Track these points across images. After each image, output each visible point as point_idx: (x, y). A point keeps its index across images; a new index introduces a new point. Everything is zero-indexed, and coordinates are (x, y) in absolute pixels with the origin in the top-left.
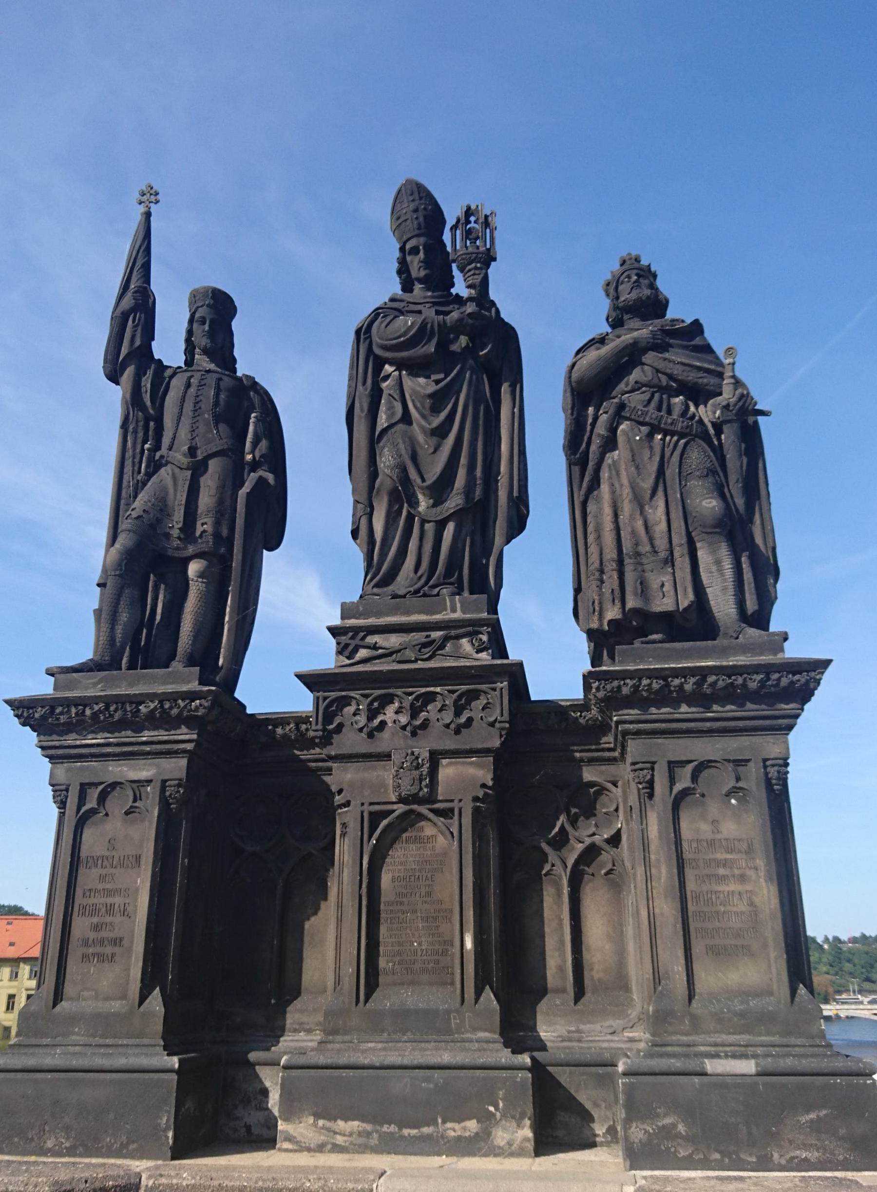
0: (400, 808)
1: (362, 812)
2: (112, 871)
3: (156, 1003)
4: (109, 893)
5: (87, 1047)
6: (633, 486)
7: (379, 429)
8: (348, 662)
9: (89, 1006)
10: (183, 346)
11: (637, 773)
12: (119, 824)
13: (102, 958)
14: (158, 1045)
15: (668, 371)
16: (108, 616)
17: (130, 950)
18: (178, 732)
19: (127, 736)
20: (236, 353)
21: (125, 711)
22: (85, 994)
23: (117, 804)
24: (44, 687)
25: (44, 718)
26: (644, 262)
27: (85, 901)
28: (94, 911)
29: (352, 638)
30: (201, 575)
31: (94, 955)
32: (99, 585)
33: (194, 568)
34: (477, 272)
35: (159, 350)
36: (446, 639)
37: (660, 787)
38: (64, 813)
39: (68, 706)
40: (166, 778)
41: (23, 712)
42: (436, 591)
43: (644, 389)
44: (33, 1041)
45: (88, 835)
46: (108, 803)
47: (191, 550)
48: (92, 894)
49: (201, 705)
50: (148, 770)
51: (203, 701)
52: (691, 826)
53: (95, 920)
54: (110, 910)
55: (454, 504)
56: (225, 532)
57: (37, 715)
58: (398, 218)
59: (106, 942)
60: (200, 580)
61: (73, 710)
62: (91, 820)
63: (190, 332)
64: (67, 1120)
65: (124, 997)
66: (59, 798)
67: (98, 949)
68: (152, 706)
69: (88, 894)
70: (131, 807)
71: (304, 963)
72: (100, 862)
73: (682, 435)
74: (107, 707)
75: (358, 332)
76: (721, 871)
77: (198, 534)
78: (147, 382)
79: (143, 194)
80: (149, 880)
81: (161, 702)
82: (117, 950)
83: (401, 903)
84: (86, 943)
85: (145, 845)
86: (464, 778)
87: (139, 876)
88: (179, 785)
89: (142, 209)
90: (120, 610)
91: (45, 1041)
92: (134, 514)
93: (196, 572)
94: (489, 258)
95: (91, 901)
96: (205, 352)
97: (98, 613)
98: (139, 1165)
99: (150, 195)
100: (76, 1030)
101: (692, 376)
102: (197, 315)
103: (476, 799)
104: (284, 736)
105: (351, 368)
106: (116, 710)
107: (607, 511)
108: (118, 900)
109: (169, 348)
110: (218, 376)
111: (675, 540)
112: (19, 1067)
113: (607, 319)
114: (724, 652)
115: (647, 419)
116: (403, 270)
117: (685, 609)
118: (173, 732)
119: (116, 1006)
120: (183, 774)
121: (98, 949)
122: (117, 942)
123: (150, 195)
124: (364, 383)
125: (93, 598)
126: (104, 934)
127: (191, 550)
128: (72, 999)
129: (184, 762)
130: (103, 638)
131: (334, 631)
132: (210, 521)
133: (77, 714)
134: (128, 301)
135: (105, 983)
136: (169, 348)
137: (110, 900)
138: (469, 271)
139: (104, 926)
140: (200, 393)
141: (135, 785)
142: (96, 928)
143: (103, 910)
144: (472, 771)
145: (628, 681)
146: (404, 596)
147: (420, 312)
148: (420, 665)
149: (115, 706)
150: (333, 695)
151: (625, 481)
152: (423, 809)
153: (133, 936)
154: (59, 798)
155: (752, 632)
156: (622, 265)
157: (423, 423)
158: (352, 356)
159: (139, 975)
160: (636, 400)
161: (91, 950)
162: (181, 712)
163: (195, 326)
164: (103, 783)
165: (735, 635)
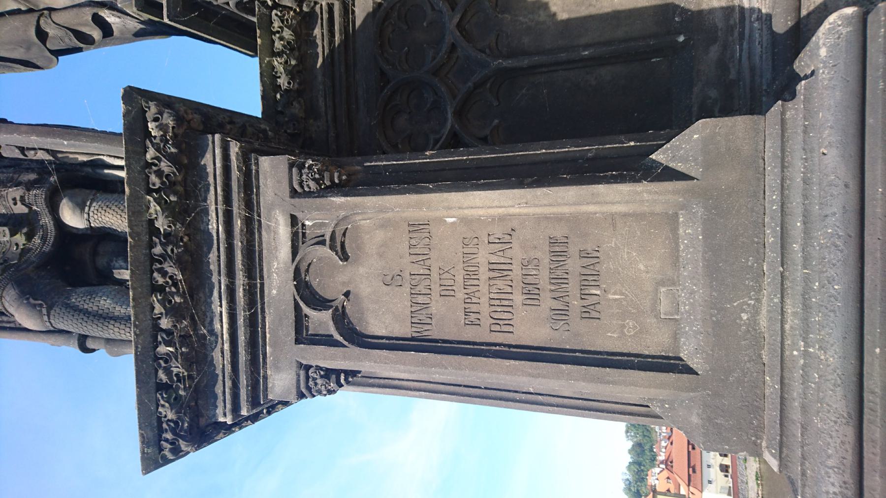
2: (435, 275)
3: (682, 149)
4: (471, 275)
5: (788, 284)
9: (692, 293)
12: (362, 270)
13: (590, 278)
14: (783, 113)
17: (574, 221)
18: (210, 169)
19: (215, 259)
21: (164, 257)
22: (664, 306)
23: (331, 280)
25: (176, 403)
27: (486, 322)
28: (501, 302)
30: (81, 206)
39: (156, 358)
41: (167, 440)
44: (771, 414)
45: (376, 326)
46: (326, 293)
47: (46, 220)
48: (474, 308)
49: (156, 120)
50: (277, 223)
51: (150, 115)
53: (518, 298)
54: (499, 271)
57: (171, 415)
60: (87, 209)
61: (163, 349)
62: (354, 321)
65: (672, 220)
66: (319, 381)
67: (573, 287)
68: (154, 207)
70: (332, 248)
71: (620, 8)
72: (420, 299)
74: (161, 289)
77: (26, 210)
80: (446, 195)
81: (149, 192)
82: (573, 250)
84: (561, 314)
85: (390, 215)
87: (441, 221)
90: (95, 308)
91: (771, 385)
93: (74, 212)
95: (485, 309)
100: (745, 316)
104: (292, 74)
106: (164, 273)
108: (483, 257)
112: (850, 432)
118: (211, 179)
119: (690, 231)
121: (573, 287)
122: (558, 249)
126: (543, 278)
127: (46, 220)
128: (675, 337)
129: (265, 162)
133: (168, 344)
135: (641, 267)
137: (484, 274)
139: (530, 279)
142: (532, 293)
143: (500, 284)
149: (155, 274)
153: (546, 218)
154: (319, 381)
159: (624, 189)
161: (576, 303)
162: (171, 158)
164: (297, 307)
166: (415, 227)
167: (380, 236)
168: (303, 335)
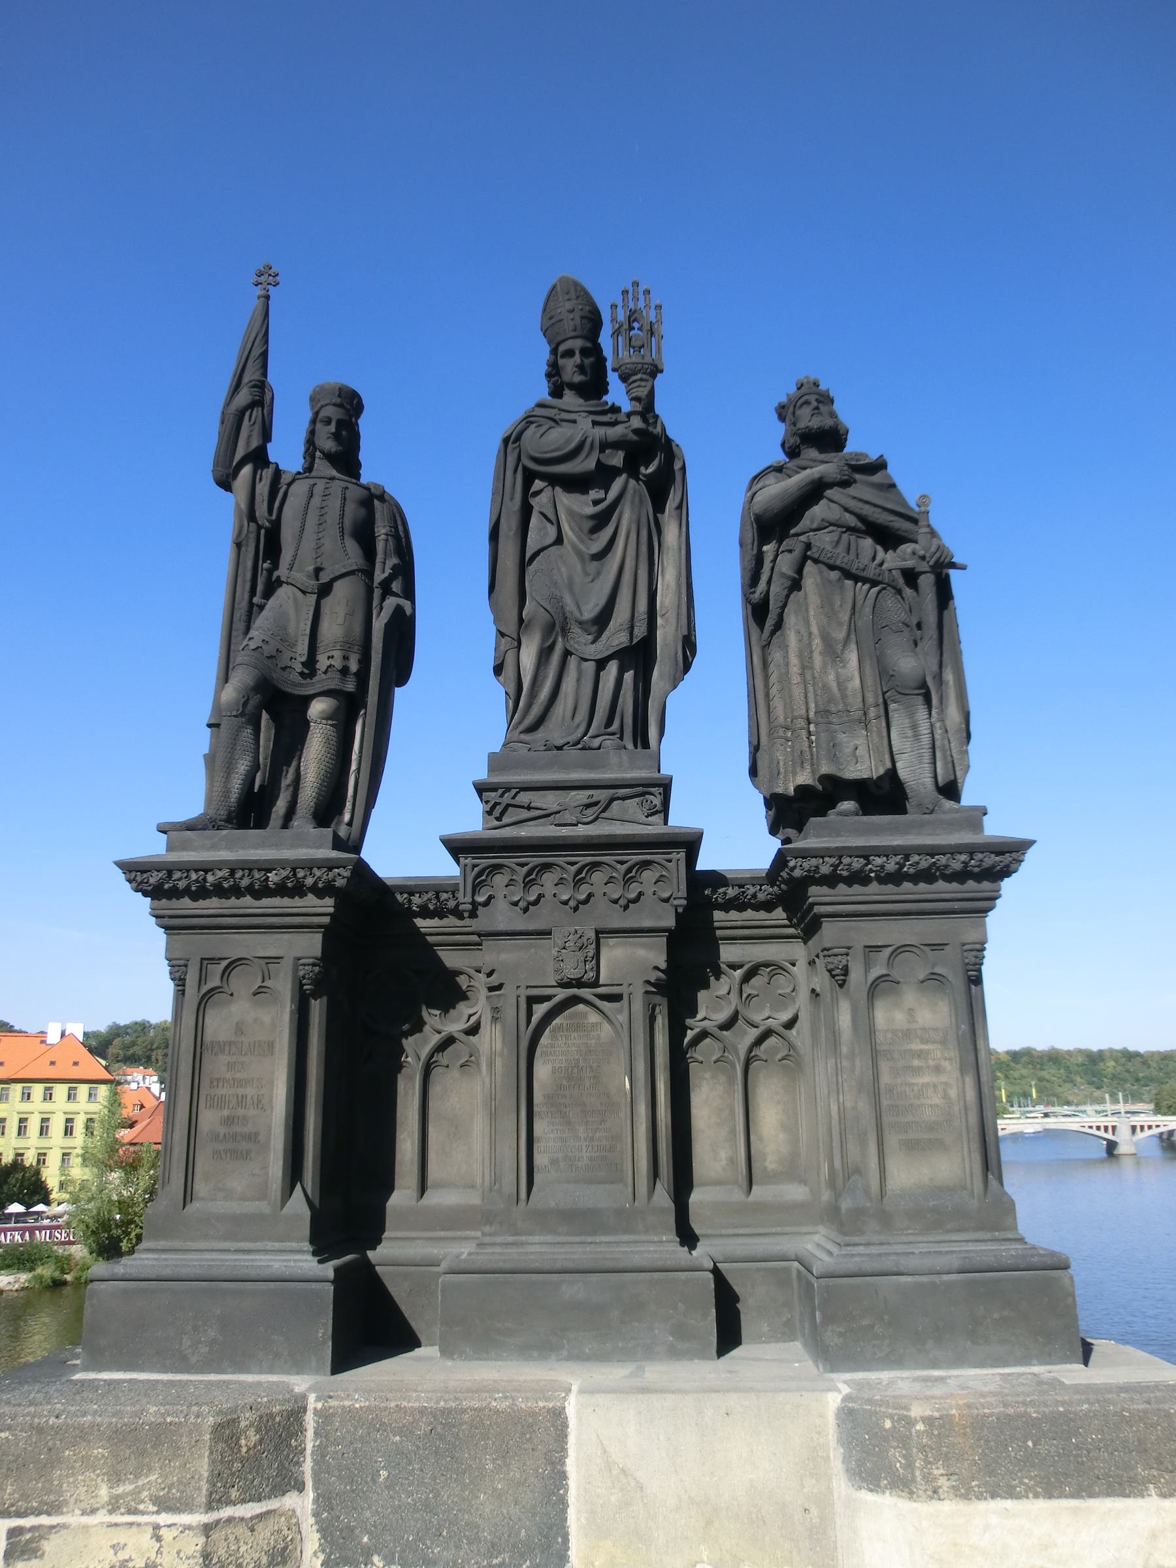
0: (562, 994)
1: (518, 997)
4: (240, 1083)
6: (826, 638)
8: (496, 823)
10: (302, 449)
11: (829, 960)
15: (859, 512)
17: (266, 1147)
20: (361, 457)
23: (243, 983)
26: (823, 387)
29: (502, 796)
30: (329, 717)
31: (226, 1151)
32: (209, 726)
33: (318, 708)
34: (643, 384)
35: (275, 452)
36: (612, 800)
37: (856, 975)
38: (183, 992)
40: (299, 955)
42: (596, 742)
43: (831, 528)
48: (221, 1084)
52: (888, 1016)
53: (226, 1113)
54: (241, 1101)
55: (617, 642)
56: (354, 667)
57: (152, 881)
58: (551, 318)
59: (239, 1138)
63: (312, 433)
69: (215, 1083)
73: (874, 583)
75: (506, 441)
78: (263, 488)
81: (294, 870)
83: (564, 1096)
84: (216, 1137)
86: (634, 961)
88: (314, 965)
89: (259, 291)
92: (253, 645)
94: (655, 371)
96: (329, 457)
97: (210, 760)
99: (267, 277)
101: (882, 518)
102: (322, 414)
103: (648, 982)
105: (496, 478)
107: (794, 660)
109: (287, 451)
110: (344, 484)
111: (870, 699)
112: (153, 1276)
113: (783, 445)
114: (919, 827)
115: (838, 563)
116: (554, 371)
117: (880, 778)
120: (318, 952)
122: (252, 1137)
123: (267, 277)
124: (512, 499)
125: (203, 740)
128: (202, 1199)
129: (318, 938)
130: (218, 786)
132: (337, 654)
134: (244, 397)
136: (287, 451)
137: (240, 1091)
138: (635, 381)
140: (325, 504)
141: (263, 962)
144: (642, 953)
145: (827, 859)
146: (560, 748)
147: (574, 422)
148: (581, 830)
150: (484, 863)
151: (815, 630)
152: (585, 993)
155: (949, 804)
156: (799, 389)
157: (581, 547)
158: (497, 467)
160: (824, 541)
163: (319, 426)
165: (931, 807)
166: (271, 1045)
167: (267, 1019)
168: (207, 961)
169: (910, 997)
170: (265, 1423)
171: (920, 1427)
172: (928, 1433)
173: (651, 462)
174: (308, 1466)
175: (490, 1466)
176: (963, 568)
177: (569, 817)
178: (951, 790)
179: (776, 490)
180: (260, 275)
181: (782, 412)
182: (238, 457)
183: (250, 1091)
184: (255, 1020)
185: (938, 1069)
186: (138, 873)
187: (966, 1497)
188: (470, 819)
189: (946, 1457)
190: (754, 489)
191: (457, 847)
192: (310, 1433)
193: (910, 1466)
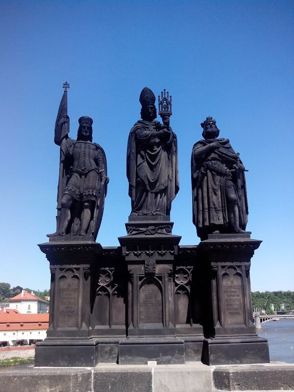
7: (138, 164)
16: (59, 219)
24: (46, 241)
64: (66, 358)
76: (233, 294)
79: (64, 84)
89: (64, 89)
98: (89, 368)
99: (66, 85)
107: (205, 195)
123: (66, 85)
126: (69, 310)
131: (127, 225)
136: (73, 135)
155: (243, 231)
169: (232, 278)
170: (83, 375)
171: (231, 374)
172: (233, 376)
173: (168, 142)
174: (92, 386)
175: (134, 385)
176: (248, 171)
177: (148, 233)
178: (243, 226)
179: (201, 148)
180: (64, 84)
181: (203, 125)
182: (62, 137)
183: (72, 301)
184: (73, 283)
185: (238, 296)
186: (43, 248)
187: (241, 390)
188: (124, 234)
189: (237, 381)
190: (196, 148)
191: (121, 240)
192: (93, 378)
193: (229, 383)
